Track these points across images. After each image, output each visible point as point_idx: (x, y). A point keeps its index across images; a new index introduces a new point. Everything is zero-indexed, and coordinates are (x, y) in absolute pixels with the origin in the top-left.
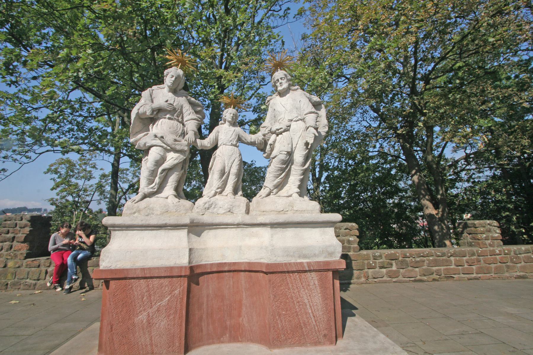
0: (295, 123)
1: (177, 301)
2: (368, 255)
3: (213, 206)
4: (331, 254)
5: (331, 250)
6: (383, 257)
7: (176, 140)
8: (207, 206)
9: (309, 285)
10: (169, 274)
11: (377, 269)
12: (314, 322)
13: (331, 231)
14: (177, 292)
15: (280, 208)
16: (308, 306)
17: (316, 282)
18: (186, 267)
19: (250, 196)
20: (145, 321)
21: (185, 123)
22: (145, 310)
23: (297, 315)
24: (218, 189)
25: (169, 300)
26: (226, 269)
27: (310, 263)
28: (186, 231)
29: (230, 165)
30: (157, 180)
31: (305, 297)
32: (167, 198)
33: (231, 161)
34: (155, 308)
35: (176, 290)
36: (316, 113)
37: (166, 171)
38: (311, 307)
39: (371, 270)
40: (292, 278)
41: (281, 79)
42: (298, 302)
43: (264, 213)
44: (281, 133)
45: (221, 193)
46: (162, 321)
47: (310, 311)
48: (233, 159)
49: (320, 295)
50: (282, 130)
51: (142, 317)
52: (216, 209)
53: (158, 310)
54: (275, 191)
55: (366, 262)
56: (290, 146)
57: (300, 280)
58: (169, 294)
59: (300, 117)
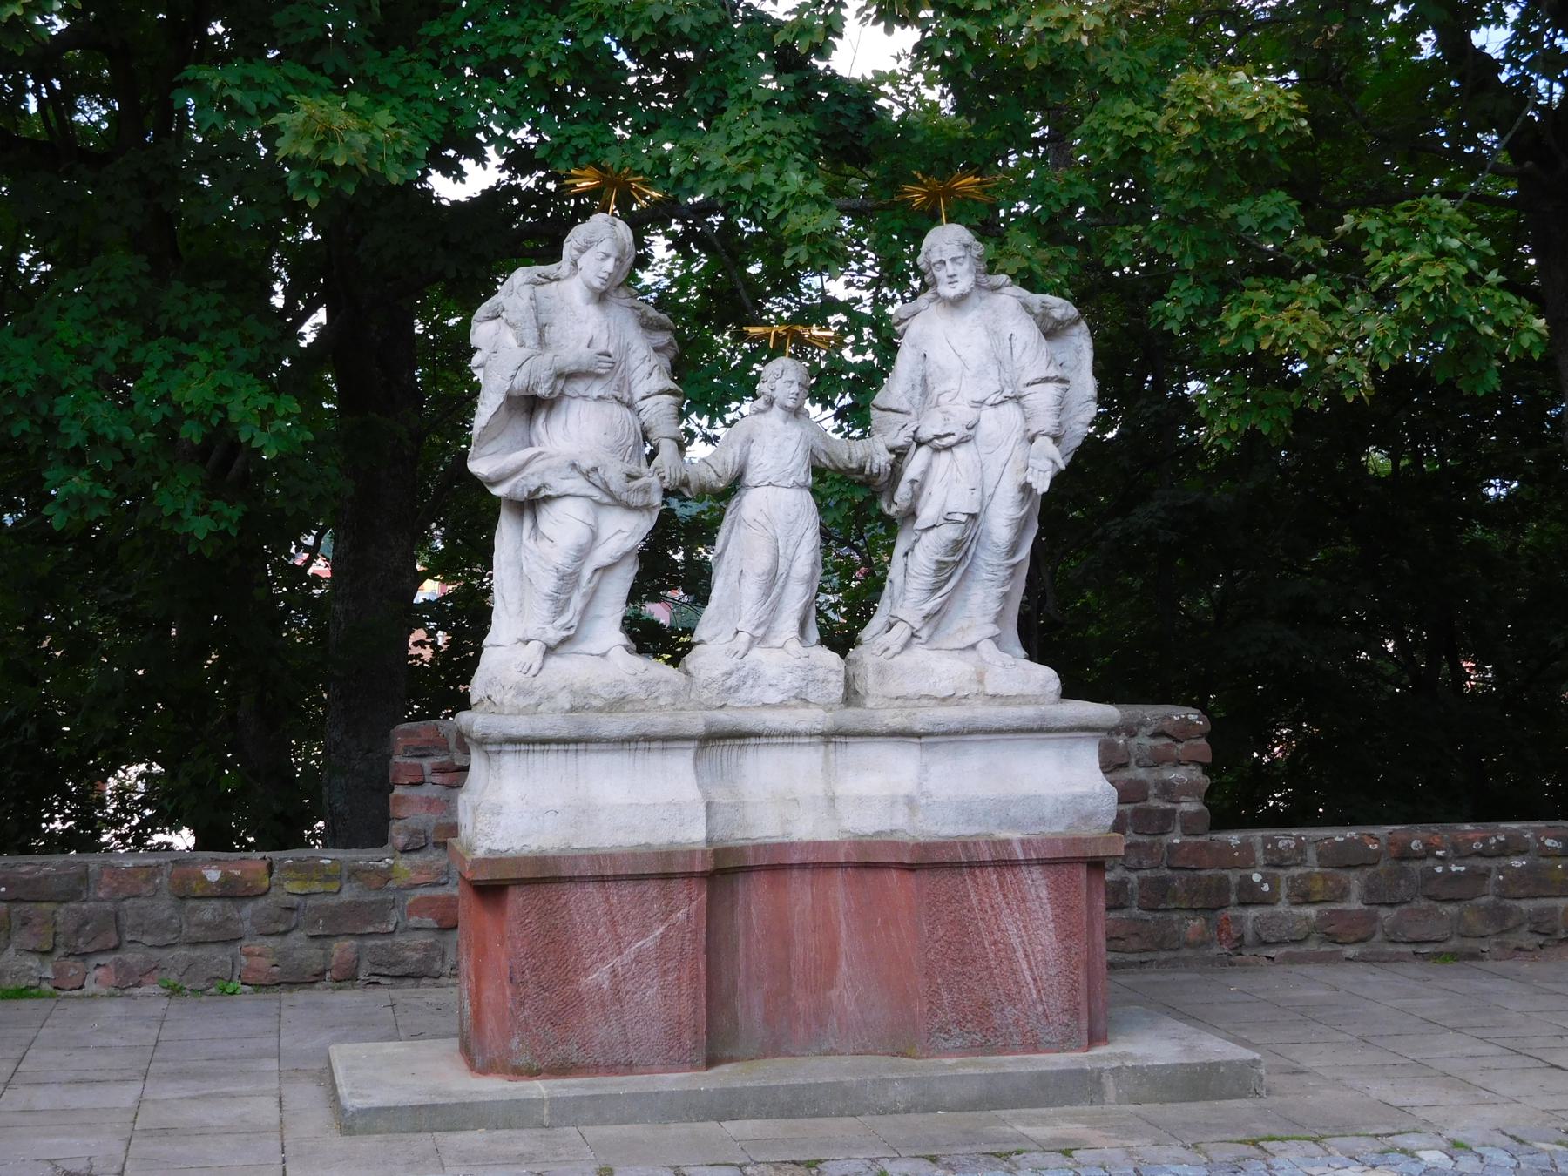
0: (992, 411)
1: (683, 938)
2: (1246, 847)
3: (750, 682)
4: (1087, 818)
5: (1089, 805)
6: (1311, 855)
7: (631, 477)
8: (732, 681)
9: (1024, 901)
10: (656, 872)
11: (1281, 908)
12: (1034, 992)
13: (1087, 758)
14: (681, 915)
15: (944, 688)
16: (1020, 954)
17: (1044, 893)
18: (704, 853)
19: (841, 640)
20: (605, 986)
21: (640, 405)
22: (603, 959)
23: (991, 976)
24: (757, 627)
25: (663, 936)
26: (796, 859)
27: (1030, 841)
28: (690, 754)
29: (790, 551)
30: (577, 602)
31: (1012, 930)
32: (604, 655)
33: (795, 538)
34: (630, 952)
35: (678, 909)
36: (1062, 381)
37: (598, 575)
38: (1027, 956)
39: (1252, 912)
40: (980, 881)
41: (953, 260)
42: (995, 943)
43: (899, 702)
44: (948, 448)
45: (763, 639)
46: (649, 986)
47: (1025, 966)
48: (799, 533)
49: (1051, 926)
50: (951, 440)
51: (599, 976)
52: (757, 690)
53: (637, 961)
54: (924, 634)
55: (1234, 877)
56: (977, 494)
57: (1001, 886)
58: (663, 921)
59: (1008, 392)
